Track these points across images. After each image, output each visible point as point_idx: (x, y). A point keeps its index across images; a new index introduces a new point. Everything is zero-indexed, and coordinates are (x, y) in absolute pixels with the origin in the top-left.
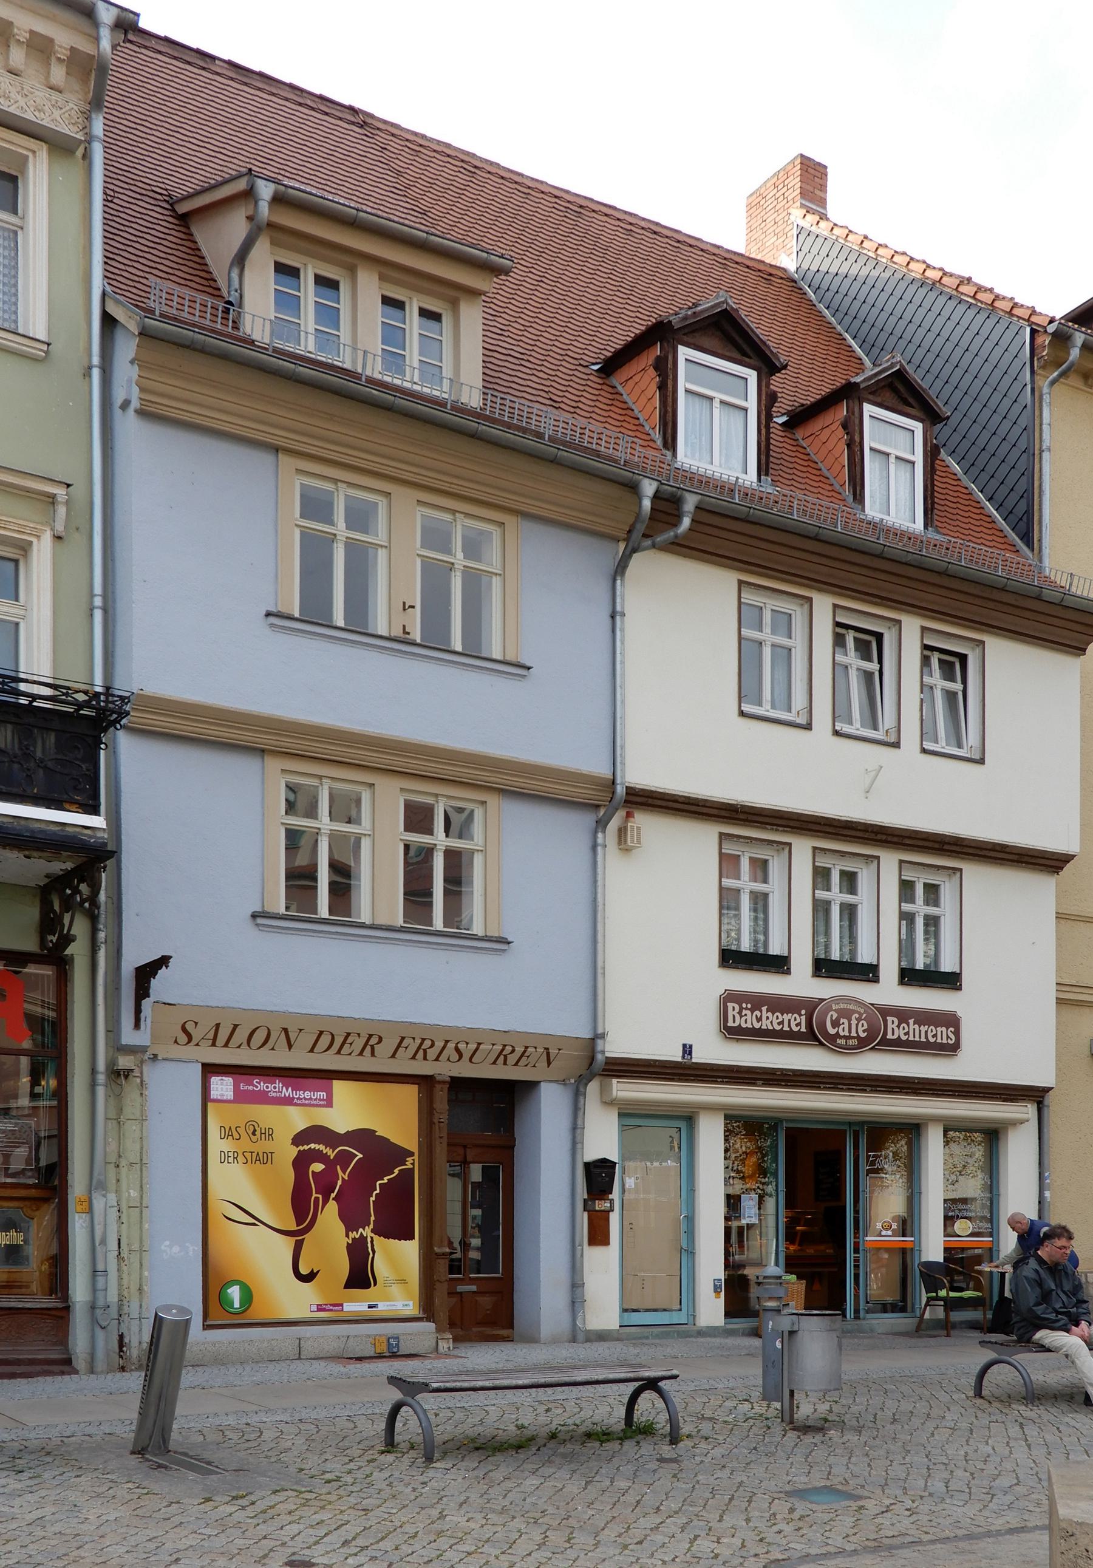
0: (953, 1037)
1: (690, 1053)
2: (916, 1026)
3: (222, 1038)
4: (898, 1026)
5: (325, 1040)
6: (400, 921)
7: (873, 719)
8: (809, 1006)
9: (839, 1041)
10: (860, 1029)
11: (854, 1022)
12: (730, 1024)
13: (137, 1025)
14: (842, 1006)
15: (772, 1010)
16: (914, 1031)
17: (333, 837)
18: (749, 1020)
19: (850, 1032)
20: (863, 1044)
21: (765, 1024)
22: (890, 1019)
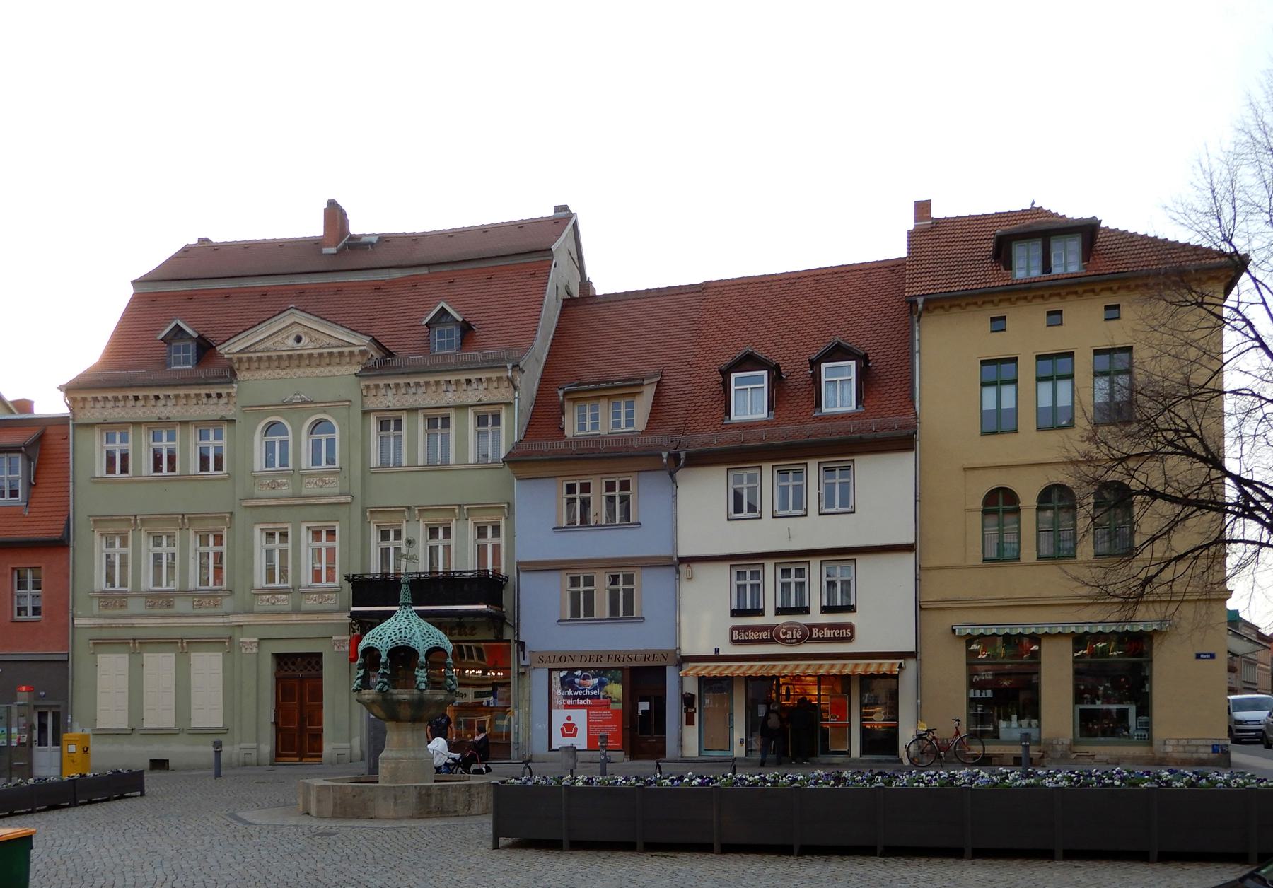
0: (849, 633)
1: (718, 651)
2: (828, 631)
3: (552, 661)
4: (818, 632)
5: (584, 659)
6: (607, 616)
7: (844, 502)
8: (771, 628)
9: (787, 641)
10: (798, 635)
11: (794, 632)
12: (734, 638)
13: (524, 659)
14: (788, 626)
18: (743, 636)
19: (792, 636)
20: (798, 642)
21: (751, 637)
22: (814, 629)
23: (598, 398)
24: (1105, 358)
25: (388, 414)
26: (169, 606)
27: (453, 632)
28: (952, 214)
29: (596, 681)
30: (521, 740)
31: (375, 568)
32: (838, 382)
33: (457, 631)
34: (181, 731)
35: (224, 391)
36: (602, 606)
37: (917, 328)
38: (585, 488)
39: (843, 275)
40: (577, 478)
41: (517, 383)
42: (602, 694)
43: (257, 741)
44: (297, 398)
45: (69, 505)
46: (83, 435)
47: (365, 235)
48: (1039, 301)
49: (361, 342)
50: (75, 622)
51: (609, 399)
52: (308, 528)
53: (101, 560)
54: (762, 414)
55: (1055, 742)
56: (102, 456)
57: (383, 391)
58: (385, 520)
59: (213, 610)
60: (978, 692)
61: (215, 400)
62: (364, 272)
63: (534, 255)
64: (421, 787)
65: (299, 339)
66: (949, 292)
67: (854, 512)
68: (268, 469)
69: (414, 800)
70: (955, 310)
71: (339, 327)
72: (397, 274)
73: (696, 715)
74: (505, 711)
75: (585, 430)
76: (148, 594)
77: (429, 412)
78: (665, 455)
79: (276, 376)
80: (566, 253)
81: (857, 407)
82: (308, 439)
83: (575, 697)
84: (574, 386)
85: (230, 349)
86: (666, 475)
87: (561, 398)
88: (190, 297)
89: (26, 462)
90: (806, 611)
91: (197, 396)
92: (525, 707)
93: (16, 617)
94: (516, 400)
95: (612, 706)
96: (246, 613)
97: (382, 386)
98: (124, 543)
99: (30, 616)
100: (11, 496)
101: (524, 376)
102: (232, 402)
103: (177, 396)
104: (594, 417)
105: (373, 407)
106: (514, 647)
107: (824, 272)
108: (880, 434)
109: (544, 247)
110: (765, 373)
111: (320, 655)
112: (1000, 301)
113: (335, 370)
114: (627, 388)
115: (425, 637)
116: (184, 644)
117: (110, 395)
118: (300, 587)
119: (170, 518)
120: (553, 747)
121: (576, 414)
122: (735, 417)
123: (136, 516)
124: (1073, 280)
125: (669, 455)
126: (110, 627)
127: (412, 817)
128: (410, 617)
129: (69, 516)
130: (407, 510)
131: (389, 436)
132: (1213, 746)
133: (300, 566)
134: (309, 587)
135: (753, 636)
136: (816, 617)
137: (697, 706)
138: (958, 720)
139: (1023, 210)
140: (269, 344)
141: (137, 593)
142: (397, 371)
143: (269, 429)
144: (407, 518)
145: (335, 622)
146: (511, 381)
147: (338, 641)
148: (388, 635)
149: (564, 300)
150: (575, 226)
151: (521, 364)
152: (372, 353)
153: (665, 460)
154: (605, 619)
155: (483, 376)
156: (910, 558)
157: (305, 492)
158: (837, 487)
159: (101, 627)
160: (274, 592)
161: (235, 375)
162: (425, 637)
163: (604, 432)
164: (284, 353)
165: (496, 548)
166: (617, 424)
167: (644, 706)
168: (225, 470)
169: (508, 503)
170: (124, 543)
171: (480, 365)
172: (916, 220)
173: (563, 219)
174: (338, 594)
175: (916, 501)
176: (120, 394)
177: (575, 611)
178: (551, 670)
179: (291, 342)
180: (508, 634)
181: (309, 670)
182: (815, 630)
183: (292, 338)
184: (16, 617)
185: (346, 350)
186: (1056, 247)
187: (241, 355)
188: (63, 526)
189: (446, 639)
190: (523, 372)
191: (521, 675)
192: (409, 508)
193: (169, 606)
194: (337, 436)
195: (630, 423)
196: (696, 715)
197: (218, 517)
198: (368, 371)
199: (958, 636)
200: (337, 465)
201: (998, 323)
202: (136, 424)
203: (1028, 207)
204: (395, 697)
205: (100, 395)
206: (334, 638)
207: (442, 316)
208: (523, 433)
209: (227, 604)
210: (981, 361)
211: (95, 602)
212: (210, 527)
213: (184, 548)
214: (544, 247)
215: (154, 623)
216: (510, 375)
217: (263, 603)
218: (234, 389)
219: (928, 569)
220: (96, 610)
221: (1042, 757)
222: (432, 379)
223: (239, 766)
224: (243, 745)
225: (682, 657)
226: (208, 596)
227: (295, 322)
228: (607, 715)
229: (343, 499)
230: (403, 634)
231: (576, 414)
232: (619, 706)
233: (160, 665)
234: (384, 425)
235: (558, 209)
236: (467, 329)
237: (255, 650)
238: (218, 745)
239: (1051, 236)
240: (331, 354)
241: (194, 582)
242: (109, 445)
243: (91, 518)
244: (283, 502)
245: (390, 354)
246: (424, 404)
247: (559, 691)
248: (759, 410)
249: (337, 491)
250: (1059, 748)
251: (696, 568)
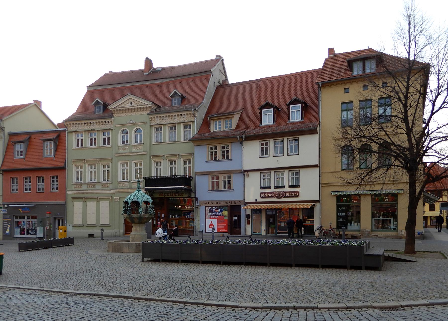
7: (296, 151)
15: (267, 194)
16: (290, 194)
17: (216, 181)
18: (264, 196)
20: (282, 197)
21: (266, 196)
23: (221, 119)
24: (345, 105)
25: (158, 126)
26: (94, 187)
28: (341, 52)
29: (220, 210)
30: (197, 229)
31: (154, 175)
32: (296, 111)
33: (177, 194)
34: (97, 225)
35: (110, 120)
36: (221, 186)
37: (320, 93)
38: (216, 148)
39: (304, 74)
40: (213, 145)
41: (196, 115)
42: (222, 214)
43: (119, 229)
44: (131, 122)
45: (66, 157)
46: (69, 134)
47: (158, 68)
48: (360, 82)
49: (149, 104)
50: (68, 192)
51: (224, 119)
52: (134, 162)
53: (75, 173)
54: (272, 122)
55: (365, 230)
56: (75, 142)
57: (156, 119)
58: (157, 159)
59: (106, 188)
60: (341, 214)
61: (107, 123)
62: (154, 81)
63: (205, 73)
64: (137, 243)
65: (131, 103)
66: (330, 80)
67: (298, 154)
68: (136, 143)
69: (135, 247)
70: (333, 86)
71: (143, 99)
72: (164, 81)
73: (250, 221)
74: (193, 221)
75: (227, 128)
76: (88, 183)
77: (170, 125)
78: (238, 137)
79: (125, 115)
80: (219, 71)
81: (301, 120)
82: (134, 135)
83: (213, 215)
84: (216, 115)
85: (111, 107)
86: (239, 143)
87: (209, 119)
88: (103, 91)
89: (54, 143)
90: (284, 187)
91: (102, 122)
93: (51, 191)
94: (196, 121)
95: (225, 218)
96: (116, 189)
97: (155, 117)
98: (81, 168)
99: (55, 190)
100: (21, 156)
101: (198, 113)
102: (112, 124)
103: (96, 122)
104: (220, 125)
105: (153, 124)
106: (194, 200)
107: (299, 73)
108: (306, 129)
109: (207, 70)
110: (272, 109)
112: (347, 83)
113: (142, 113)
114: (229, 115)
115: (142, 198)
116: (98, 199)
117: (77, 122)
118: (132, 181)
119: (94, 160)
120: (207, 231)
121: (225, 123)
122: (263, 124)
123: (85, 160)
124: (353, 78)
125: (240, 137)
126: (77, 194)
127: (134, 252)
128: (139, 192)
129: (66, 160)
131: (158, 133)
132: (418, 232)
133: (131, 174)
134: (134, 181)
135: (267, 195)
136: (287, 189)
137: (250, 218)
138: (331, 223)
139: (365, 49)
140: (123, 105)
141: (85, 183)
142: (160, 112)
143: (137, 130)
146: (194, 115)
148: (131, 197)
149: (217, 86)
150: (222, 61)
151: (197, 109)
152: (153, 107)
153: (238, 139)
154: (222, 190)
155: (186, 113)
156: (317, 170)
157: (133, 151)
158: (294, 146)
159: (75, 194)
160: (124, 182)
161: (113, 115)
162: (142, 198)
163: (222, 130)
164: (127, 108)
165: (190, 167)
166: (227, 127)
167: (235, 218)
168: (110, 145)
169: (193, 153)
170: (81, 168)
171: (184, 110)
172: (329, 55)
173: (219, 60)
174: (143, 183)
175: (320, 150)
176: (80, 122)
177: (213, 188)
178: (206, 207)
179: (129, 104)
180: (193, 195)
182: (287, 193)
183: (130, 103)
184: (51, 191)
185: (145, 106)
186: (368, 64)
187: (114, 109)
188: (64, 163)
189: (149, 197)
190: (198, 111)
191: (196, 208)
192: (164, 155)
193: (94, 187)
194: (142, 133)
195: (230, 127)
196: (250, 221)
197: (108, 159)
198: (151, 113)
199: (333, 195)
200: (143, 142)
201: (347, 90)
202: (85, 131)
203: (367, 48)
204: (132, 216)
205: (74, 123)
207: (175, 94)
208: (198, 131)
209: (111, 186)
210: (341, 103)
211: (73, 186)
212: (106, 162)
213: (85, 170)
214: (209, 70)
215: (89, 192)
216: (193, 113)
217: (121, 186)
218: (113, 119)
219: (324, 173)
220: (73, 189)
221: (361, 235)
222: (170, 115)
223: (114, 236)
224: (115, 230)
225: (246, 202)
226: (105, 184)
227: (130, 98)
228: (223, 221)
229: (144, 153)
230: (135, 197)
231: (225, 123)
232: (227, 218)
233: (91, 205)
234: (157, 129)
235: (217, 56)
236: (183, 98)
237: (118, 201)
238: (102, 230)
239: (365, 60)
240: (140, 108)
241: (101, 180)
242: (78, 138)
243: (72, 161)
244: (126, 154)
245: (159, 107)
246: (168, 123)
247: (208, 213)
248: (271, 121)
249: (142, 151)
250: (366, 232)
251: (250, 173)
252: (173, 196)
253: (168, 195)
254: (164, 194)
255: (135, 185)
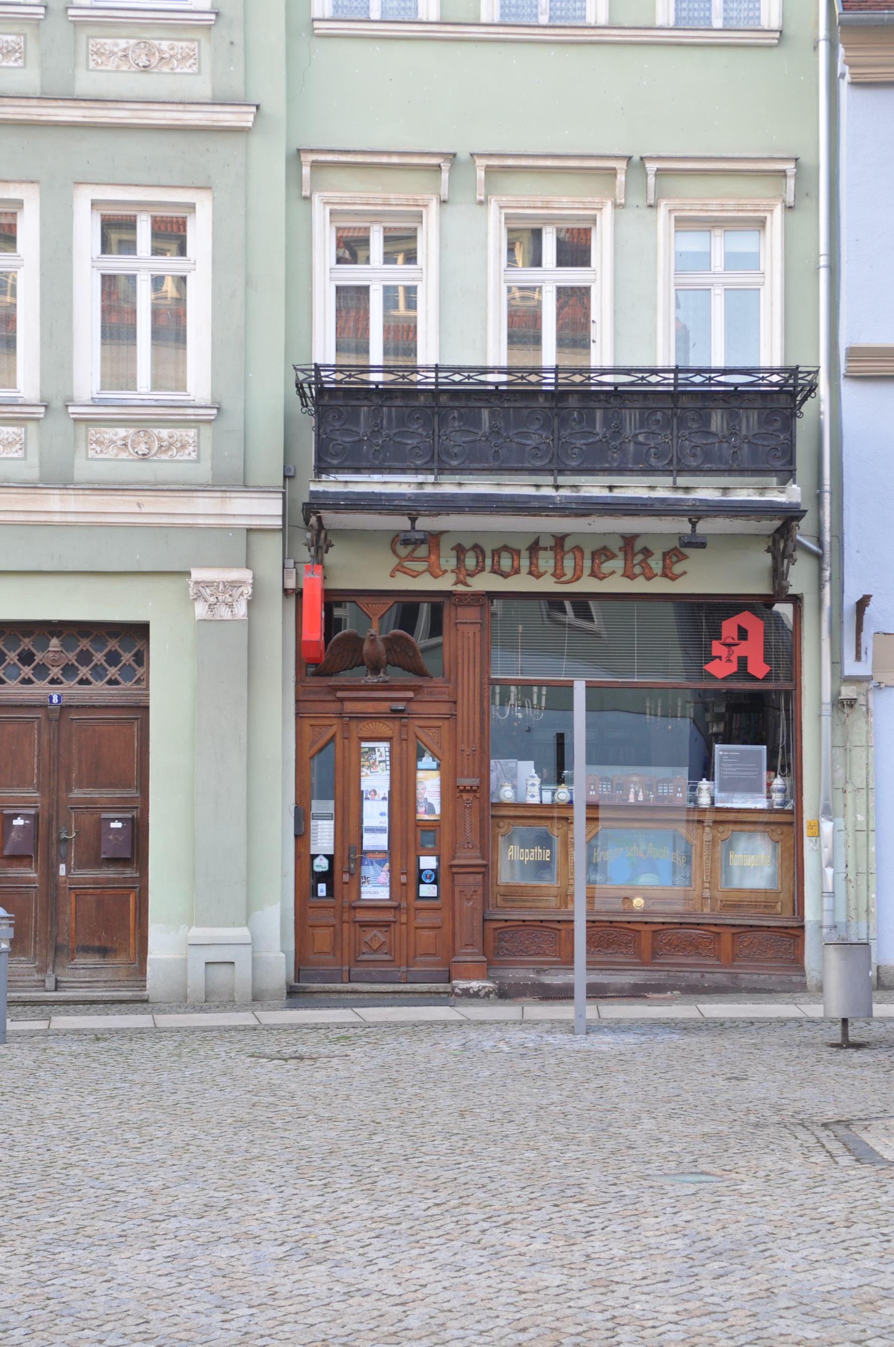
27: (607, 567)
33: (617, 564)
92: (855, 813)
111: (140, 631)
130: (445, 166)
144: (444, 192)
145: (201, 521)
147: (208, 584)
174: (206, 431)
181: (82, 682)
206: (197, 574)
229: (228, 117)
249: (203, 88)
252: (558, 575)
253: (506, 563)
254: (460, 551)
255: (111, 452)
